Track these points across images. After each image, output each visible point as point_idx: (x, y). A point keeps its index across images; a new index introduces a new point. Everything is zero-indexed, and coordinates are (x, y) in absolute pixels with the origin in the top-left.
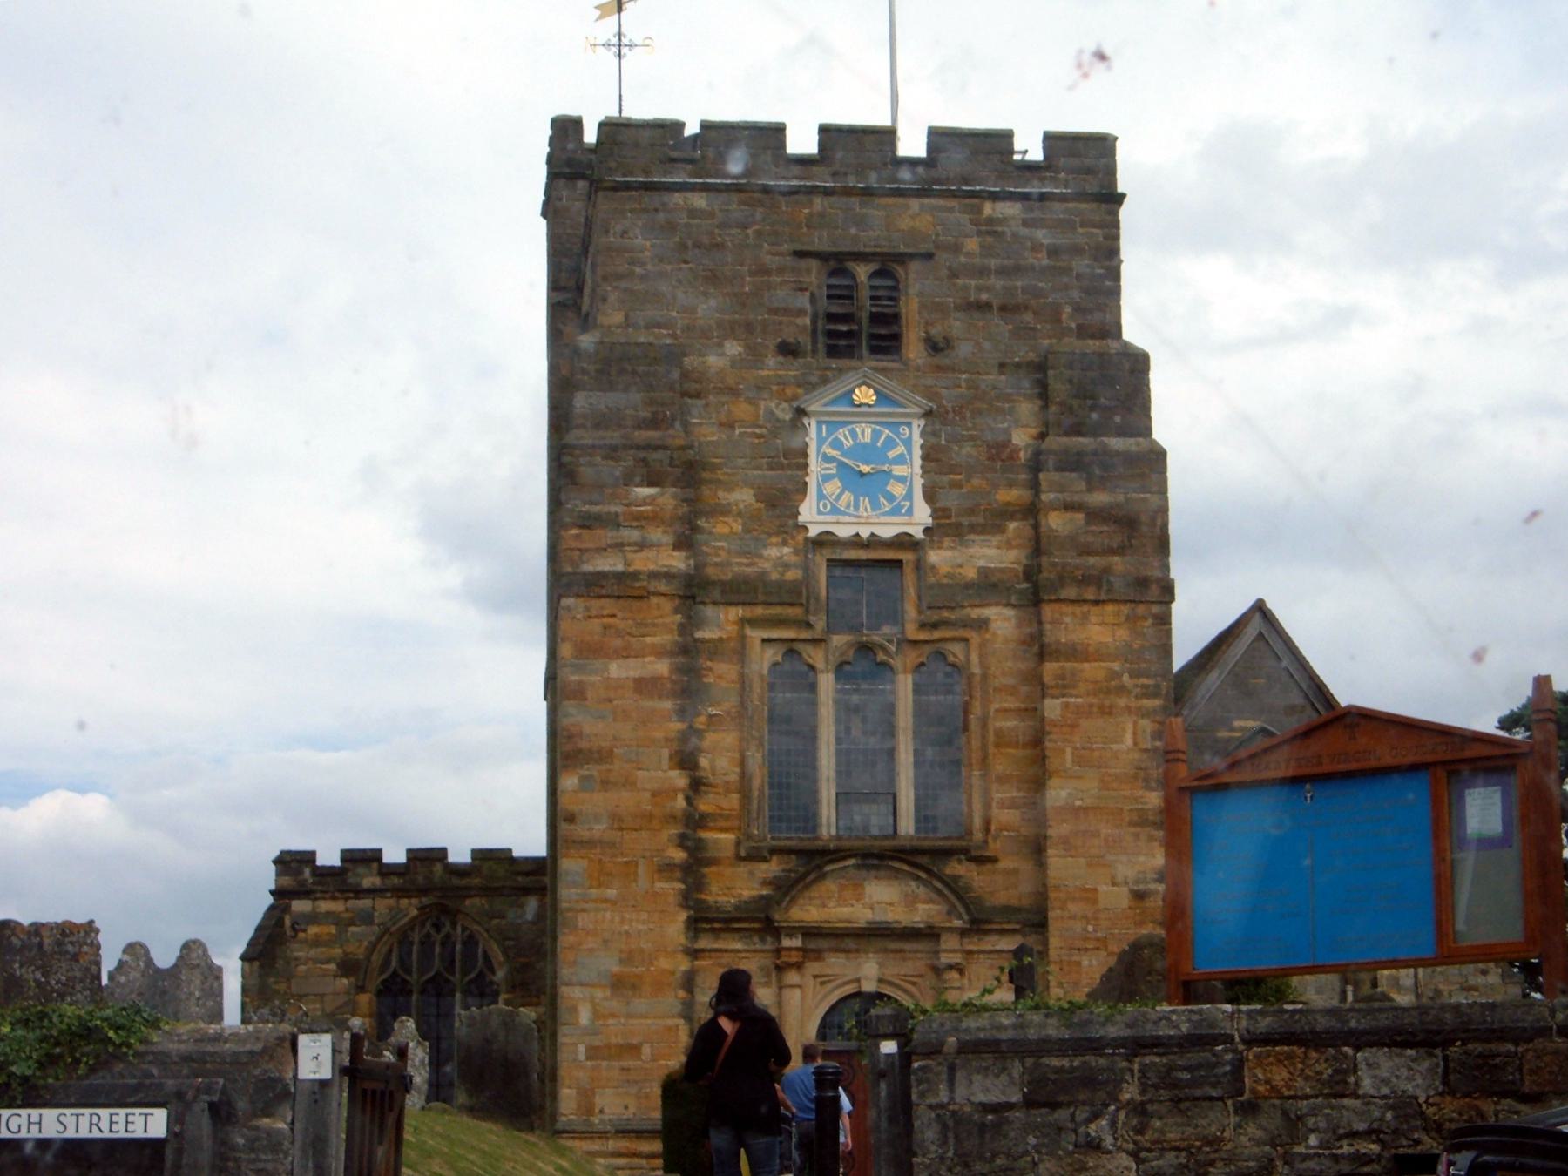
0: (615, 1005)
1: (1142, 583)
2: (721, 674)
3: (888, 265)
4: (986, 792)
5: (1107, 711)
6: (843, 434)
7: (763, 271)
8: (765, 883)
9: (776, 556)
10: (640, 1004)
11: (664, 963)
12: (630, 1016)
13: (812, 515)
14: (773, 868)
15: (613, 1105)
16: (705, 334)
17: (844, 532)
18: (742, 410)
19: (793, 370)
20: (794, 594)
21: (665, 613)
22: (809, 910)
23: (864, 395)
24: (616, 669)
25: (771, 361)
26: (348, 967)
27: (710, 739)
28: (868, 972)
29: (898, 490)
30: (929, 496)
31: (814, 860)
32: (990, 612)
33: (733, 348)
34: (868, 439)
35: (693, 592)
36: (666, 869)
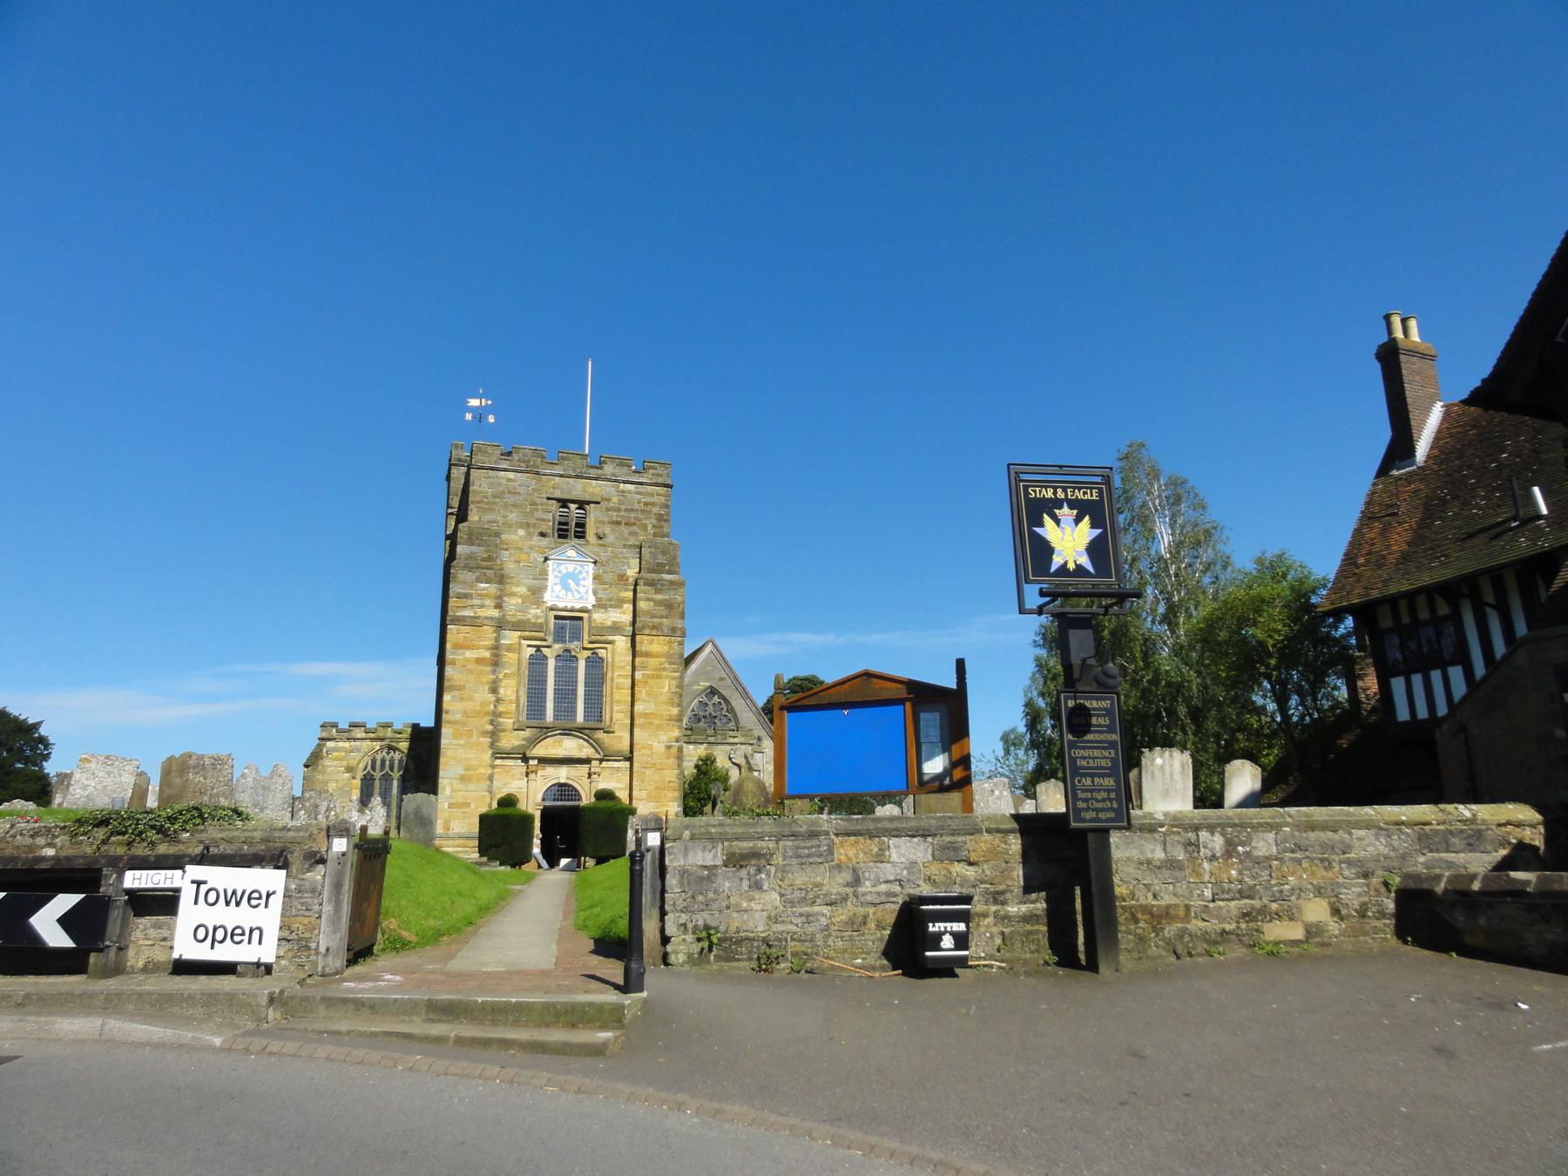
0: (460, 786)
1: (674, 629)
2: (509, 657)
3: (582, 504)
5: (660, 677)
6: (562, 568)
7: (535, 504)
9: (534, 613)
10: (471, 786)
11: (482, 771)
13: (549, 598)
14: (528, 733)
15: (457, 827)
17: (561, 605)
18: (523, 557)
19: (544, 542)
20: (538, 628)
21: (488, 633)
23: (572, 553)
24: (469, 654)
25: (536, 538)
26: (349, 769)
28: (562, 774)
29: (583, 590)
30: (595, 593)
31: (544, 731)
32: (615, 638)
33: (521, 532)
35: (501, 625)
36: (484, 733)
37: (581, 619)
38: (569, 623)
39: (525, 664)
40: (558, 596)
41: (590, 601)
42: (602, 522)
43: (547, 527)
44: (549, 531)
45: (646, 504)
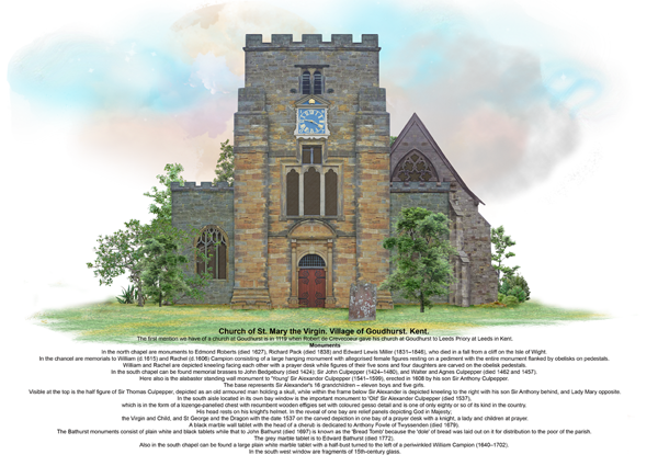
3: (319, 68)
14: (288, 223)
16: (272, 88)
18: (281, 107)
19: (295, 97)
21: (261, 157)
22: (296, 234)
27: (272, 191)
28: (312, 249)
29: (321, 126)
33: (279, 91)
38: (312, 152)
39: (285, 178)
40: (302, 131)
43: (296, 86)
44: (297, 89)
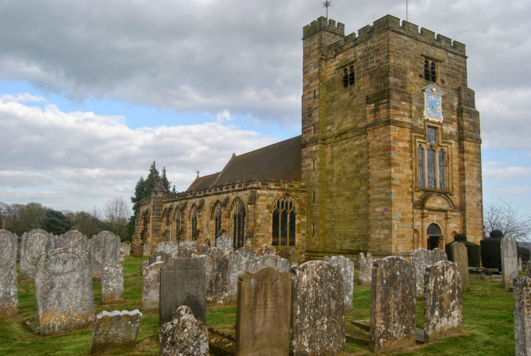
4: (452, 180)
5: (473, 166)
8: (419, 197)
10: (405, 225)
11: (409, 215)
12: (404, 228)
17: (430, 119)
25: (418, 78)
33: (412, 73)
34: (433, 99)
37: (436, 128)
41: (441, 119)
42: (443, 73)
45: (458, 66)
